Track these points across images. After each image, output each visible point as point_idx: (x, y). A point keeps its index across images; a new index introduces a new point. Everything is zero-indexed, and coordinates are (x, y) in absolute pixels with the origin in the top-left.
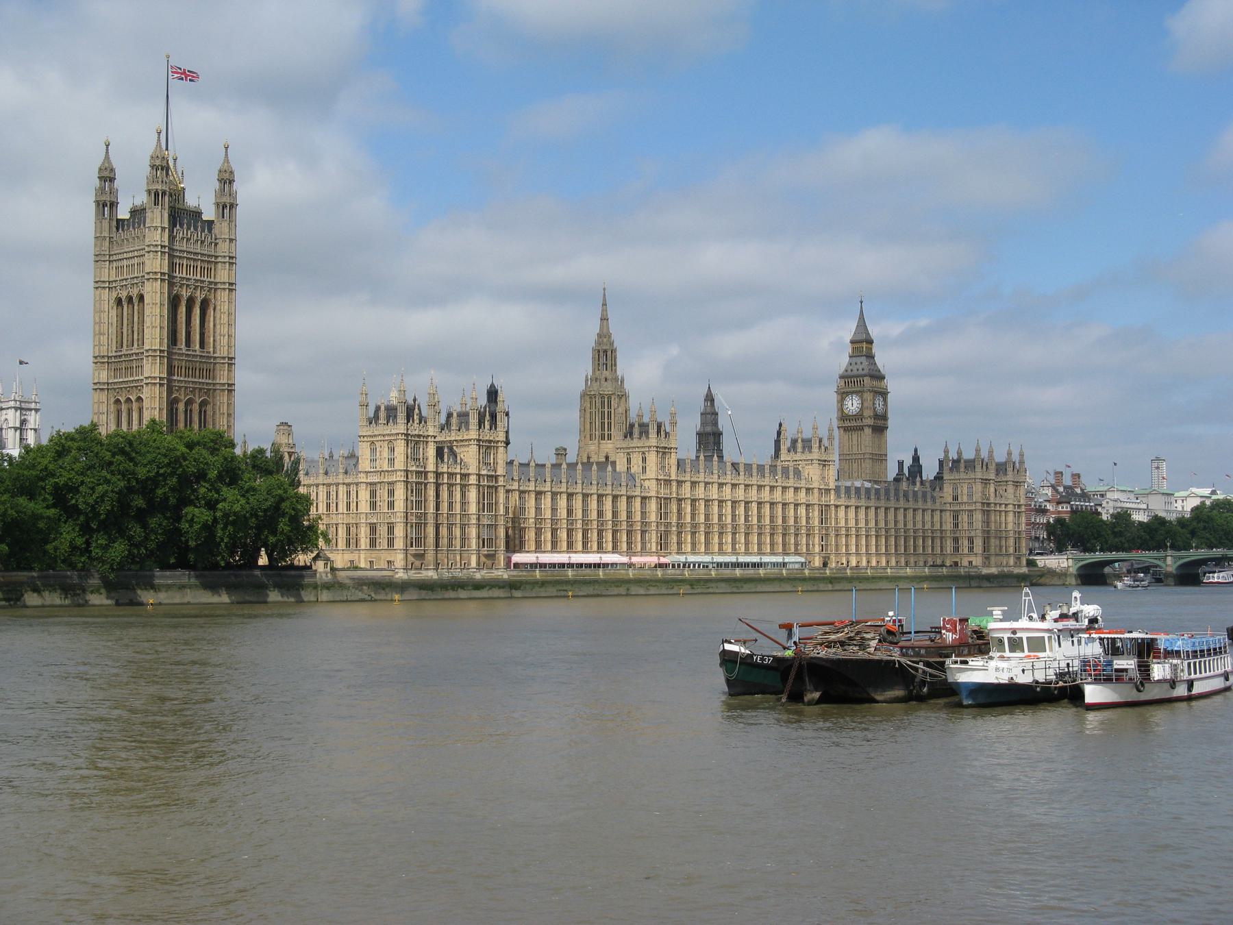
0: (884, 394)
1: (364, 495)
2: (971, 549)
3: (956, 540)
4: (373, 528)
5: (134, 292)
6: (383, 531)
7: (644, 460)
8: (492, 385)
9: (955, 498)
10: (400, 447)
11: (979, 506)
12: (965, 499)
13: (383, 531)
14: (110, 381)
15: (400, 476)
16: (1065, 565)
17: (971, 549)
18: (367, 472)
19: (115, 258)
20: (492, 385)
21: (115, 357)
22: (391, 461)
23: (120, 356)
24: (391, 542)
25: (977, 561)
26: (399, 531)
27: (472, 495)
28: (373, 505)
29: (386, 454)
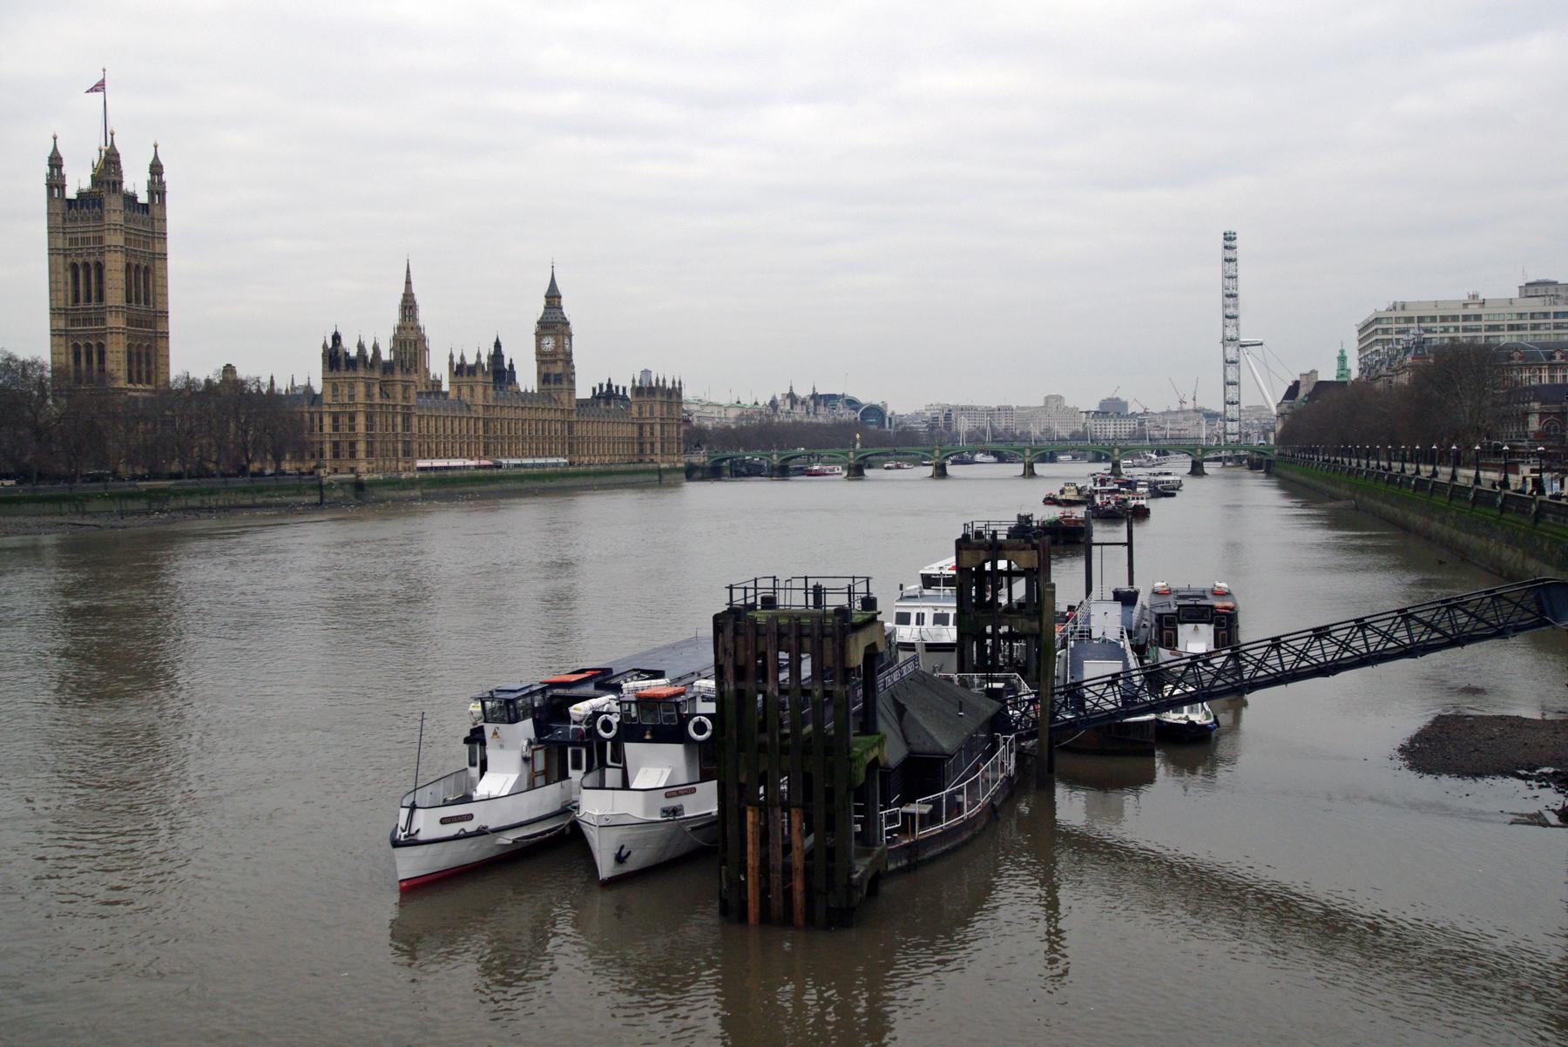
0: (570, 336)
1: (327, 421)
2: (652, 451)
3: (641, 444)
4: (336, 445)
5: (92, 260)
6: (345, 447)
7: (472, 390)
8: (336, 333)
9: (640, 413)
10: (360, 389)
11: (658, 420)
12: (648, 415)
13: (345, 447)
14: (69, 328)
15: (361, 408)
16: (702, 460)
17: (652, 451)
18: (330, 405)
19: (67, 230)
20: (336, 333)
21: (72, 310)
22: (352, 397)
23: (77, 310)
24: (353, 455)
25: (658, 459)
26: (361, 447)
27: (399, 420)
28: (336, 428)
29: (346, 391)
